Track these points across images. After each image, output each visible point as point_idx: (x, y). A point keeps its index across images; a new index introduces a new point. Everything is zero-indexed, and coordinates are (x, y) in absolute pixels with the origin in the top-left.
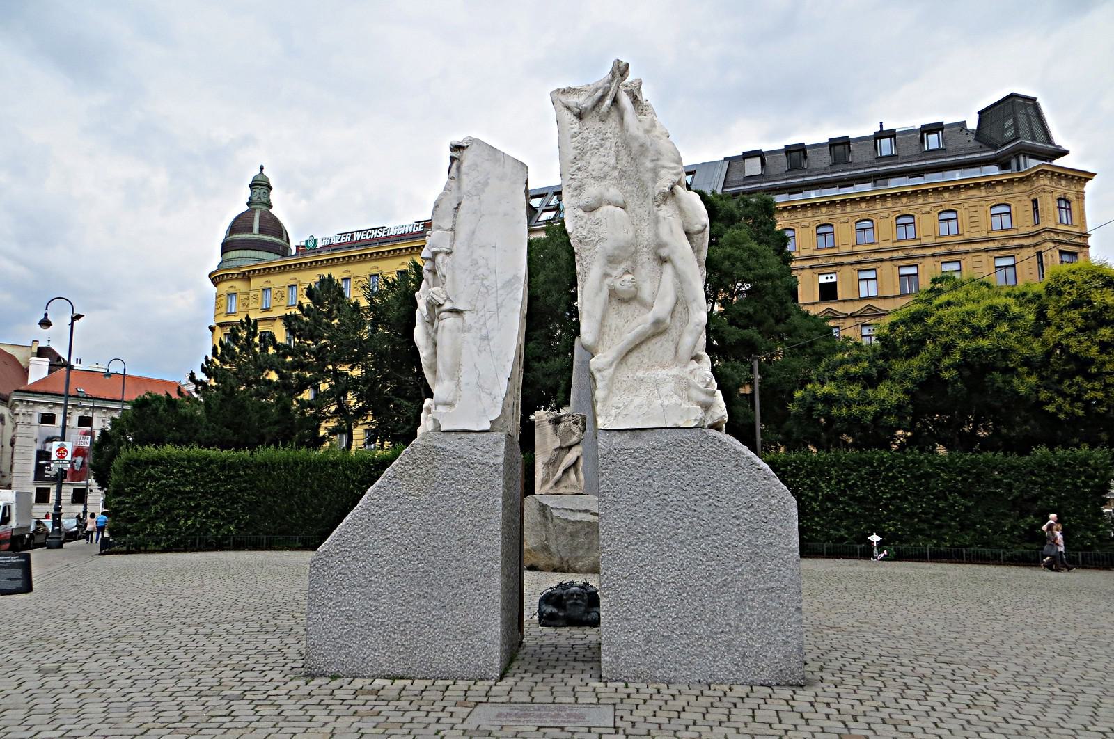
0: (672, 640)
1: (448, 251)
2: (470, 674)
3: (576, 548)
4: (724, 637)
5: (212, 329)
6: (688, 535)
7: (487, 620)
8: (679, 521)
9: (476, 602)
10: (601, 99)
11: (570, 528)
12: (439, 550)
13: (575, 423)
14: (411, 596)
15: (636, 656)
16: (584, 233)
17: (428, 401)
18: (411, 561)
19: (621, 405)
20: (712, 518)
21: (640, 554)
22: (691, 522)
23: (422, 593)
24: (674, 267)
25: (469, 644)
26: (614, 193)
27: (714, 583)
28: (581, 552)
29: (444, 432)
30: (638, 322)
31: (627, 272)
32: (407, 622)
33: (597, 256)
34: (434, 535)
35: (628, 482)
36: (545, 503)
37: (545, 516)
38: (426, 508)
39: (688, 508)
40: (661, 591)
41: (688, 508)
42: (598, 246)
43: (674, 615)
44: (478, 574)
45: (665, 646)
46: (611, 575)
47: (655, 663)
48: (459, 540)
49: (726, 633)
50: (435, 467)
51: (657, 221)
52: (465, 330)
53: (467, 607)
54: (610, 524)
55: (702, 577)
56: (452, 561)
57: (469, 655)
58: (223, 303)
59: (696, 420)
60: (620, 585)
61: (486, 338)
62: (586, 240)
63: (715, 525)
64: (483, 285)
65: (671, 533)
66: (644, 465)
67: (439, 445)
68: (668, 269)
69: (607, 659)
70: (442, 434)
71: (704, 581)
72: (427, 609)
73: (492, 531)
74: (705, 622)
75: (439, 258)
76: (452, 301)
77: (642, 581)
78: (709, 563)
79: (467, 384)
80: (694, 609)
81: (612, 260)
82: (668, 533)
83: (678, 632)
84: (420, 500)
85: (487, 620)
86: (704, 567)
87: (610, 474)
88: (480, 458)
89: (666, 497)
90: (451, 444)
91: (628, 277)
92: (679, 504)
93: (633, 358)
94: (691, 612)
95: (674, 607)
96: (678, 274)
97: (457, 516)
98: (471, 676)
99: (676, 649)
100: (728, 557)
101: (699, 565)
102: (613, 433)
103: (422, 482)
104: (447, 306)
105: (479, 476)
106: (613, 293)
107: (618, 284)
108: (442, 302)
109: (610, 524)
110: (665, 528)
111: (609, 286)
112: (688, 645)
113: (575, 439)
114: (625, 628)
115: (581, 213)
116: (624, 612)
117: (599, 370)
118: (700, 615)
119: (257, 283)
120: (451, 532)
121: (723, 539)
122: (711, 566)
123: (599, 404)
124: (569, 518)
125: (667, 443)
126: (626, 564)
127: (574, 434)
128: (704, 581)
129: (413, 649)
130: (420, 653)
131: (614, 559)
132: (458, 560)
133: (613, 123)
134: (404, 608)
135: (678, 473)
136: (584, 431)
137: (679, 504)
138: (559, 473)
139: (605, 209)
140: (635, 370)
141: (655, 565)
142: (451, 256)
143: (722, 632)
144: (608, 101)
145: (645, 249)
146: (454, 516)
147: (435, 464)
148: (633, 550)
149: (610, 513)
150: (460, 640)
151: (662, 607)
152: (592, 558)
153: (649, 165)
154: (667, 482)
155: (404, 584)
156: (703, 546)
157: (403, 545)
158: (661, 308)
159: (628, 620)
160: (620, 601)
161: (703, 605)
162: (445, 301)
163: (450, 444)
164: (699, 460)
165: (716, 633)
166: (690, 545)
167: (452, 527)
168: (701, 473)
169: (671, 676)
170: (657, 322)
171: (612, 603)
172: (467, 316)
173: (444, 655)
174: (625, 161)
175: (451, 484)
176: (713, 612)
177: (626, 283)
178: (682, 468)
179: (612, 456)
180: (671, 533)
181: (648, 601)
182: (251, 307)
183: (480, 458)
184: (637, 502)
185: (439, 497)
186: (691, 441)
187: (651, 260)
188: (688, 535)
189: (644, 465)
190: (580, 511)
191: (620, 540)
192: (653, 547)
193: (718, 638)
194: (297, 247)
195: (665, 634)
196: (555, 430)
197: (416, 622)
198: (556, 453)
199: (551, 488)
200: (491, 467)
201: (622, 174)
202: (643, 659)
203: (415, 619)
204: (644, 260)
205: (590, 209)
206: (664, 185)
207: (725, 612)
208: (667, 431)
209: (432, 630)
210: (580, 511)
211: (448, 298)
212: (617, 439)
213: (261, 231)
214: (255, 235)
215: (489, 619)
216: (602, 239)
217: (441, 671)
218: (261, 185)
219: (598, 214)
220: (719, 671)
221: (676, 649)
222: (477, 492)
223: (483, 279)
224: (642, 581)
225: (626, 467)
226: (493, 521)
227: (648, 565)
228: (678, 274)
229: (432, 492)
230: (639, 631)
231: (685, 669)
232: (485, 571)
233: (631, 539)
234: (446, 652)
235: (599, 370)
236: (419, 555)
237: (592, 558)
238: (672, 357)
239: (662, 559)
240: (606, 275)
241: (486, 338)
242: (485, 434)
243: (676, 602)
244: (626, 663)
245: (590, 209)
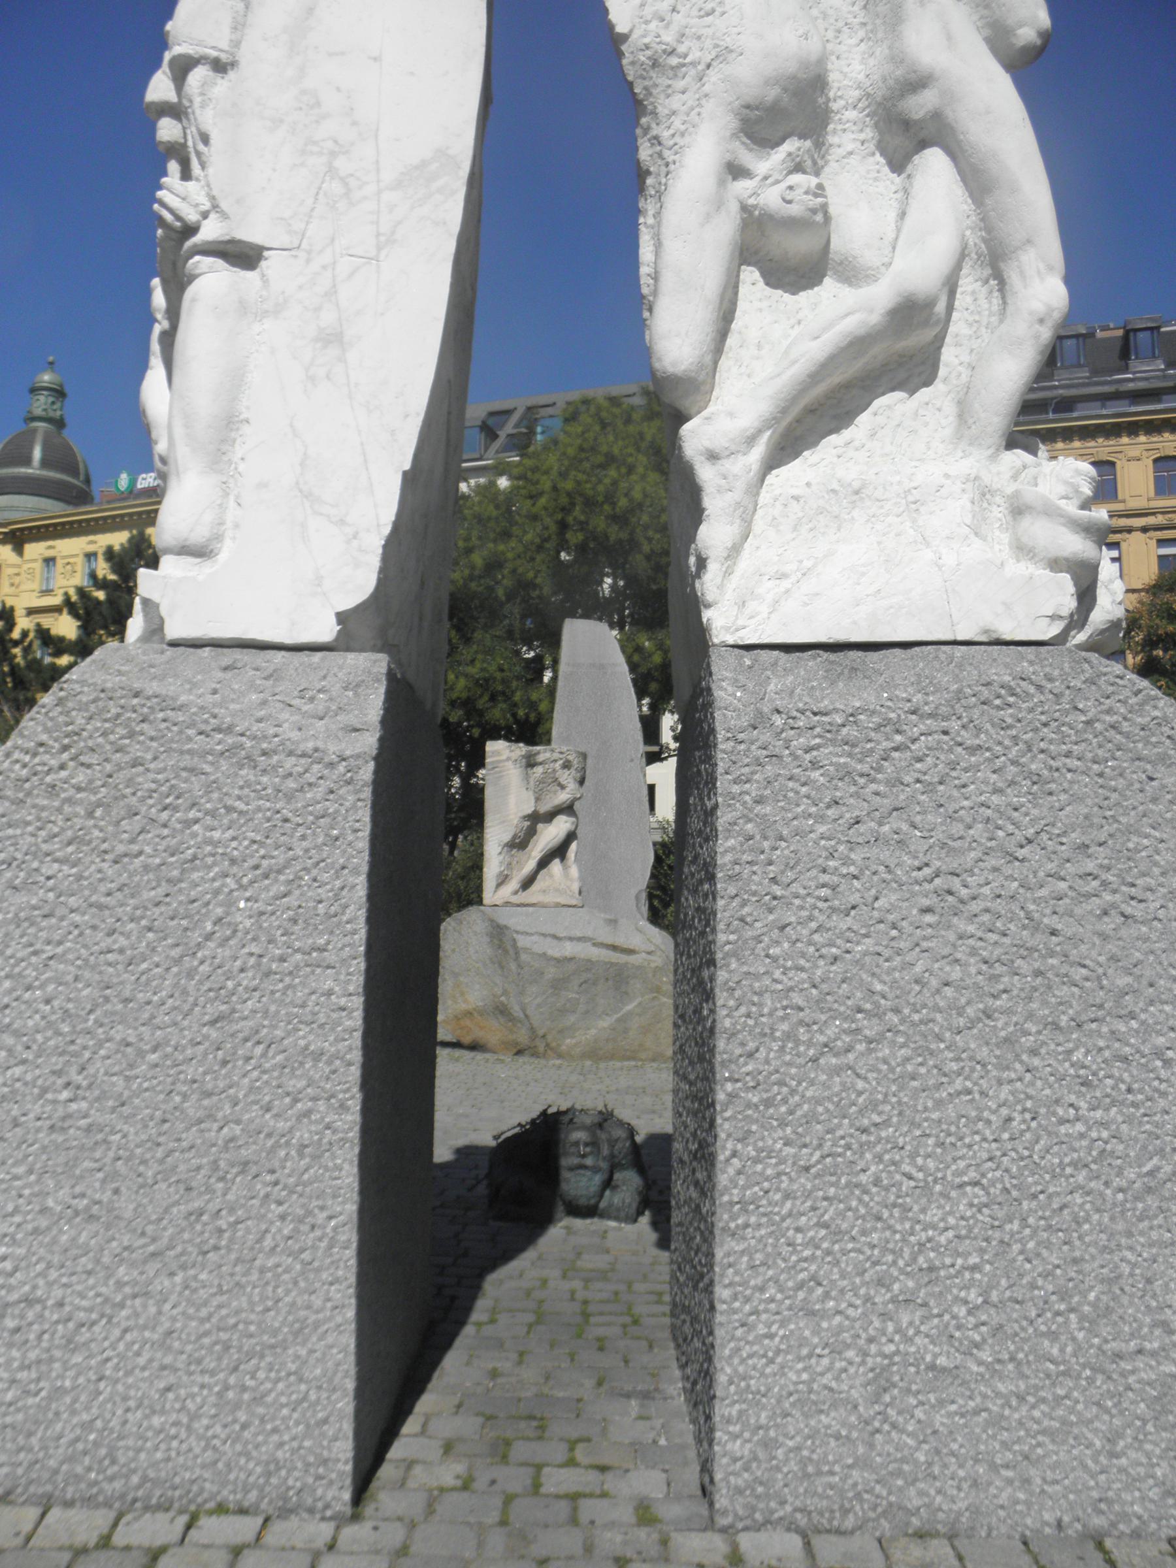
0: (964, 1383)
1: (224, 57)
2: (246, 1491)
3: (563, 1011)
4: (1145, 1370)
6: (1030, 1016)
7: (308, 1307)
8: (999, 969)
9: (268, 1242)
11: (551, 972)
12: (141, 1054)
13: (567, 765)
14: (44, 1210)
15: (838, 1437)
16: (668, 37)
18: (44, 1090)
19: (787, 568)
20: (1113, 958)
21: (860, 1084)
22: (1038, 973)
23: (82, 1203)
24: (955, 153)
25: (244, 1389)
27: (1117, 1182)
28: (572, 1019)
29: (174, 644)
31: (798, 168)
32: (29, 1301)
33: (709, 106)
34: (126, 1001)
35: (822, 829)
36: (502, 921)
37: (501, 946)
38: (101, 907)
39: (1033, 924)
40: (933, 1215)
41: (1033, 924)
42: (713, 76)
43: (973, 1296)
44: (277, 1145)
45: (941, 1403)
46: (756, 1161)
47: (903, 1460)
48: (213, 1023)
49: (1153, 1354)
50: (135, 763)
53: (238, 1261)
54: (757, 977)
55: (1073, 1164)
56: (185, 1097)
57: (244, 1427)
59: (1054, 617)
60: (787, 1196)
61: (333, 338)
62: (674, 61)
63: (1123, 981)
64: (331, 170)
65: (970, 1011)
66: (879, 770)
67: (153, 687)
68: (934, 164)
69: (736, 1447)
70: (170, 652)
71: (1081, 1177)
72: (97, 1261)
73: (330, 993)
74: (1082, 1318)
76: (224, 216)
77: (863, 1178)
78: (1099, 1114)
79: (262, 485)
80: (1046, 1275)
82: (961, 1012)
83: (986, 1355)
84: (79, 878)
85: (308, 1307)
86: (1080, 1127)
87: (759, 801)
88: (295, 735)
89: (956, 883)
90: (194, 685)
92: (999, 906)
94: (1033, 1286)
95: (974, 1268)
97: (209, 937)
98: (253, 1496)
99: (977, 1412)
100: (1164, 1094)
101: (1063, 1121)
102: (764, 654)
103: (90, 814)
104: (210, 231)
105: (289, 797)
107: (771, 198)
108: (192, 217)
109: (757, 977)
110: (949, 991)
111: (744, 208)
112: (1021, 1398)
113: (563, 797)
114: (803, 1341)
116: (800, 1286)
117: (713, 456)
118: (1063, 1295)
119: (35, 550)
120: (185, 992)
121: (1146, 1030)
122: (1103, 1125)
123: (713, 570)
124: (550, 952)
125: (959, 695)
126: (810, 1119)
127: (563, 787)
128: (1081, 1177)
129: (49, 1399)
130: (74, 1412)
131: (768, 1103)
132: (209, 1094)
134: (21, 1251)
135: (995, 799)
136: (582, 782)
137: (999, 906)
138: (531, 865)
141: (914, 1124)
142: (232, 74)
143: (1140, 1351)
145: (851, 114)
146: (196, 936)
147: (136, 750)
148: (837, 1071)
149: (758, 939)
150: (212, 1373)
151: (931, 1269)
152: (593, 1032)
154: (957, 829)
155: (21, 1170)
156: (1077, 1056)
157: (18, 1034)
159: (812, 1313)
160: (786, 1250)
161: (1075, 1261)
162: (205, 215)
164: (1068, 755)
165: (1118, 1356)
166: (1034, 1052)
167: (190, 975)
168: (1076, 799)
169: (961, 1505)
171: (759, 1258)
172: (271, 264)
173: (156, 1421)
175: (189, 823)
176: (1110, 1281)
177: (798, 195)
178: (1012, 783)
179: (766, 737)
180: (970, 1011)
181: (884, 1250)
183: (295, 735)
184: (855, 898)
185: (146, 868)
186: (1039, 688)
187: (871, 146)
188: (1030, 1016)
189: (879, 770)
190: (571, 939)
191: (788, 1036)
192: (907, 1059)
193: (1124, 1374)
195: (942, 1361)
196: (527, 778)
197: (60, 1304)
198: (527, 823)
199: (516, 893)
200: (331, 765)
202: (861, 1450)
203: (58, 1293)
204: (850, 147)
207: (1149, 1281)
208: (960, 651)
209: (117, 1332)
211: (215, 207)
212: (782, 682)
215: (317, 1302)
216: (724, 54)
217: (145, 1479)
220: (1128, 1487)
221: (977, 1412)
222: (280, 856)
223: (333, 154)
224: (863, 1178)
225: (815, 774)
226: (330, 957)
227: (886, 1123)
229: (121, 848)
230: (850, 1354)
231: (1010, 1482)
232: (303, 1134)
233: (831, 1032)
234: (163, 1412)
235: (713, 456)
236: (73, 1070)
237: (593, 1032)
238: (948, 432)
239: (939, 1104)
240: (736, 171)
241: (333, 338)
242: (317, 657)
243: (982, 1251)
244: (804, 1463)
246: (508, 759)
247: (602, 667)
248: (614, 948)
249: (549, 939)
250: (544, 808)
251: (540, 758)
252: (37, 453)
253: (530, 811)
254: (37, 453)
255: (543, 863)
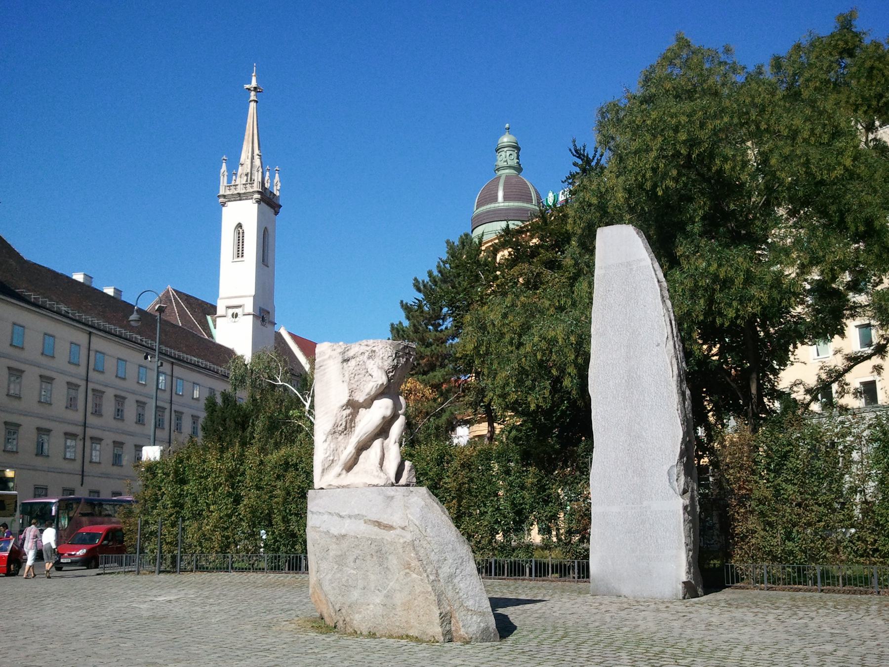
11: (334, 550)
190: (350, 517)
198: (348, 411)
210: (350, 517)
246: (330, 357)
247: (629, 264)
248: (378, 524)
249: (336, 517)
250: (360, 397)
251: (350, 354)
252: (500, 194)
253: (345, 401)
254: (500, 194)
255: (362, 447)
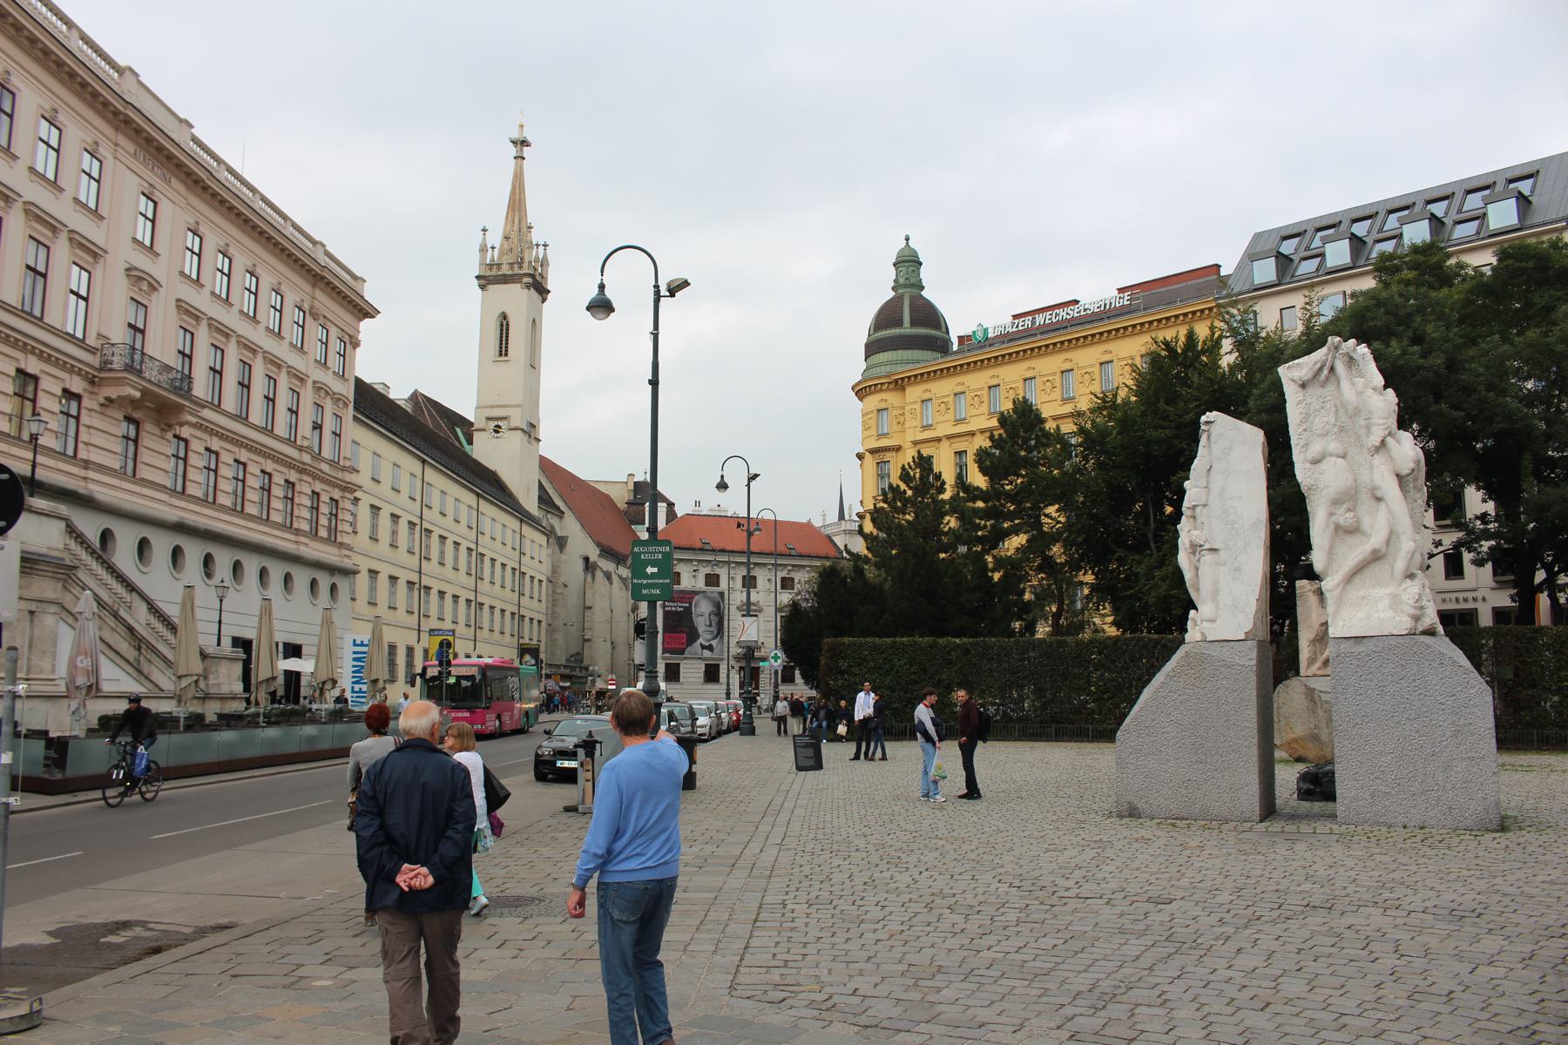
5: (860, 457)
10: (1321, 369)
17: (1192, 612)
26: (1334, 446)
30: (1355, 552)
31: (1349, 510)
37: (1312, 700)
51: (1371, 467)
52: (1218, 564)
58: (873, 423)
61: (1238, 569)
68: (1383, 506)
75: (1198, 509)
81: (1336, 502)
91: (1350, 515)
93: (1357, 580)
96: (1389, 510)
104: (1207, 546)
106: (1338, 527)
107: (1341, 521)
115: (1308, 465)
119: (914, 393)
133: (1330, 388)
139: (1330, 460)
140: (1358, 591)
144: (1326, 372)
153: (1363, 423)
158: (1376, 540)
163: (1216, 651)
170: (1374, 552)
172: (1222, 553)
174: (1344, 418)
182: (907, 425)
194: (961, 339)
201: (1342, 429)
205: (1316, 462)
206: (1375, 439)
212: (1344, 646)
213: (914, 323)
214: (907, 329)
218: (909, 262)
219: (1323, 465)
228: (1389, 510)
240: (1331, 514)
245: (1316, 462)
